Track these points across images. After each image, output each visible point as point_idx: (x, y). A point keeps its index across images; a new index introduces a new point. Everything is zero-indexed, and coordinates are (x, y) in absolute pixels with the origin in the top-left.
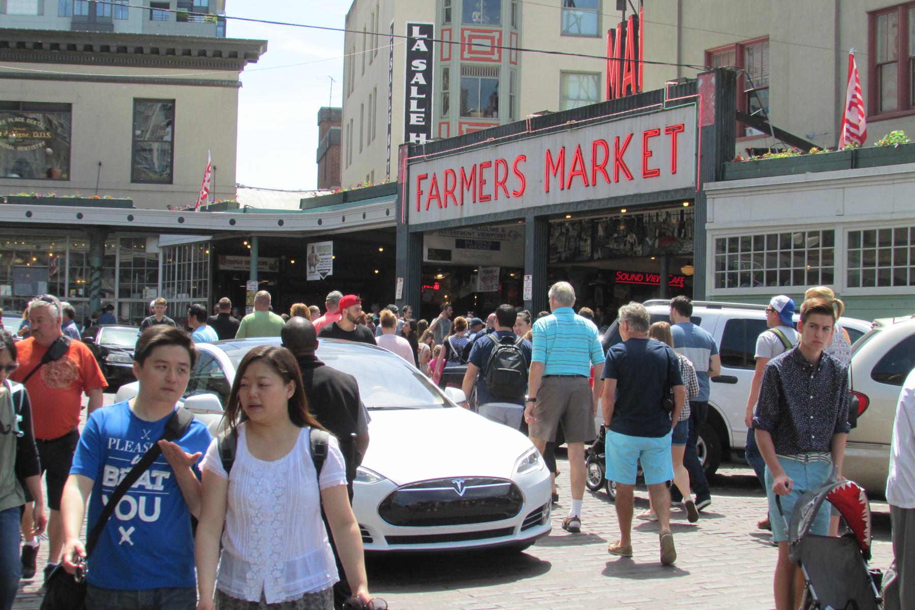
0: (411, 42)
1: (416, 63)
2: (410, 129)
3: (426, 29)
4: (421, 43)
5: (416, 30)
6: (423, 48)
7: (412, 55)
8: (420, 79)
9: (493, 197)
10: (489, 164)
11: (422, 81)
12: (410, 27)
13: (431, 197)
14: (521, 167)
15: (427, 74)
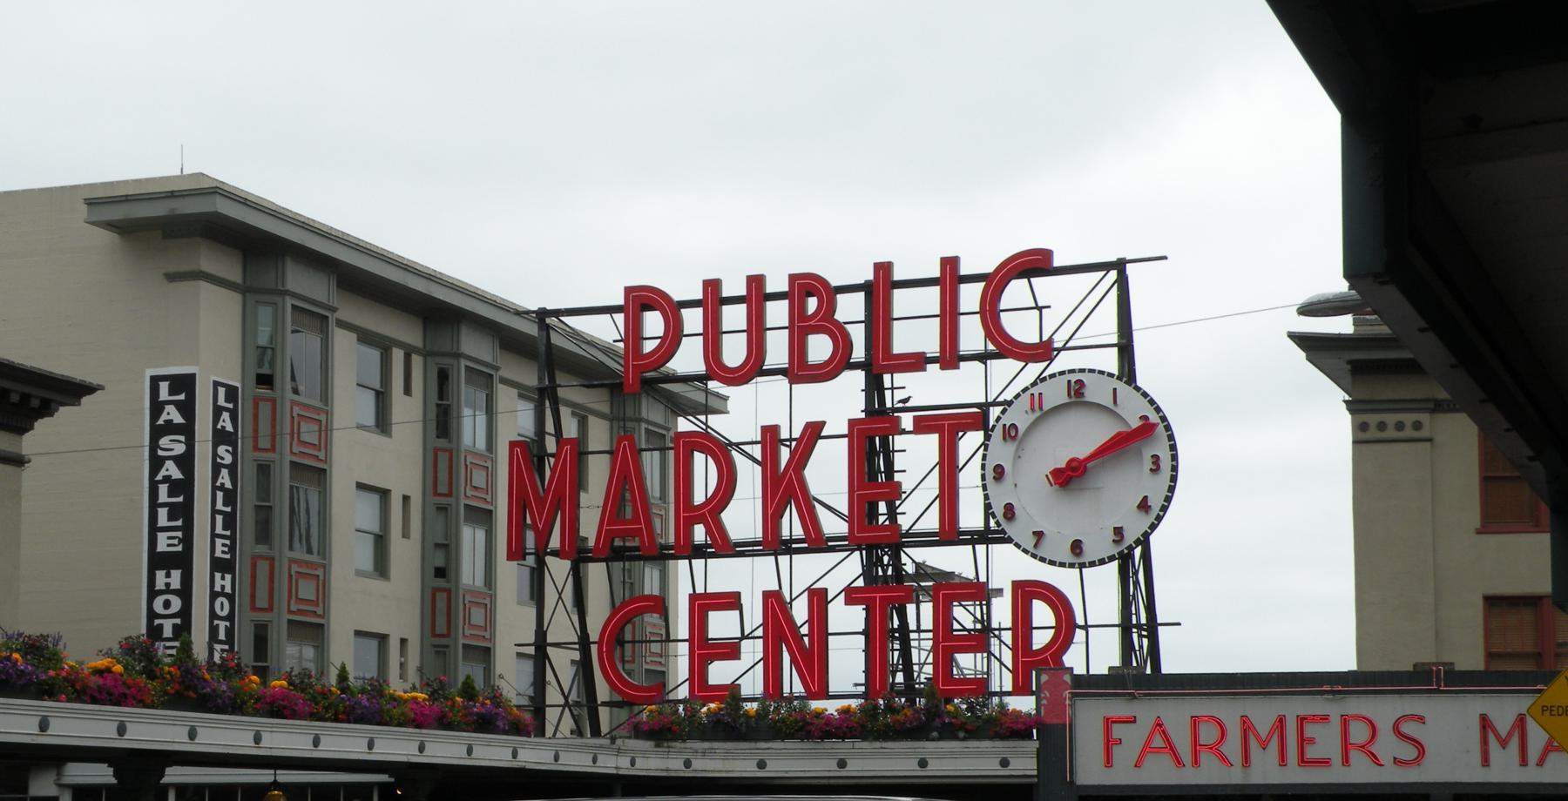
0: (218, 411)
1: (222, 450)
2: (219, 566)
3: (232, 393)
4: (226, 415)
5: (222, 391)
6: (229, 428)
7: (220, 437)
8: (225, 479)
9: (1337, 758)
10: (1325, 719)
11: (228, 485)
12: (216, 384)
13: (1147, 749)
14: (1407, 728)
15: (232, 469)
